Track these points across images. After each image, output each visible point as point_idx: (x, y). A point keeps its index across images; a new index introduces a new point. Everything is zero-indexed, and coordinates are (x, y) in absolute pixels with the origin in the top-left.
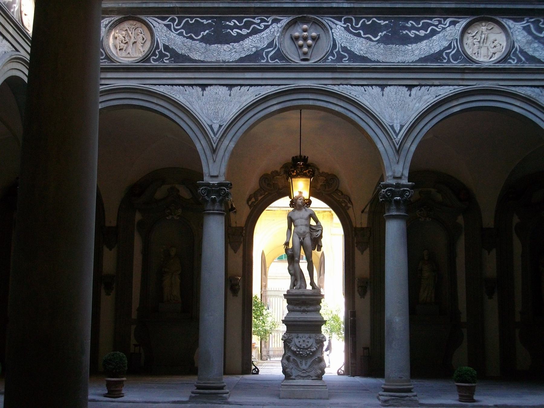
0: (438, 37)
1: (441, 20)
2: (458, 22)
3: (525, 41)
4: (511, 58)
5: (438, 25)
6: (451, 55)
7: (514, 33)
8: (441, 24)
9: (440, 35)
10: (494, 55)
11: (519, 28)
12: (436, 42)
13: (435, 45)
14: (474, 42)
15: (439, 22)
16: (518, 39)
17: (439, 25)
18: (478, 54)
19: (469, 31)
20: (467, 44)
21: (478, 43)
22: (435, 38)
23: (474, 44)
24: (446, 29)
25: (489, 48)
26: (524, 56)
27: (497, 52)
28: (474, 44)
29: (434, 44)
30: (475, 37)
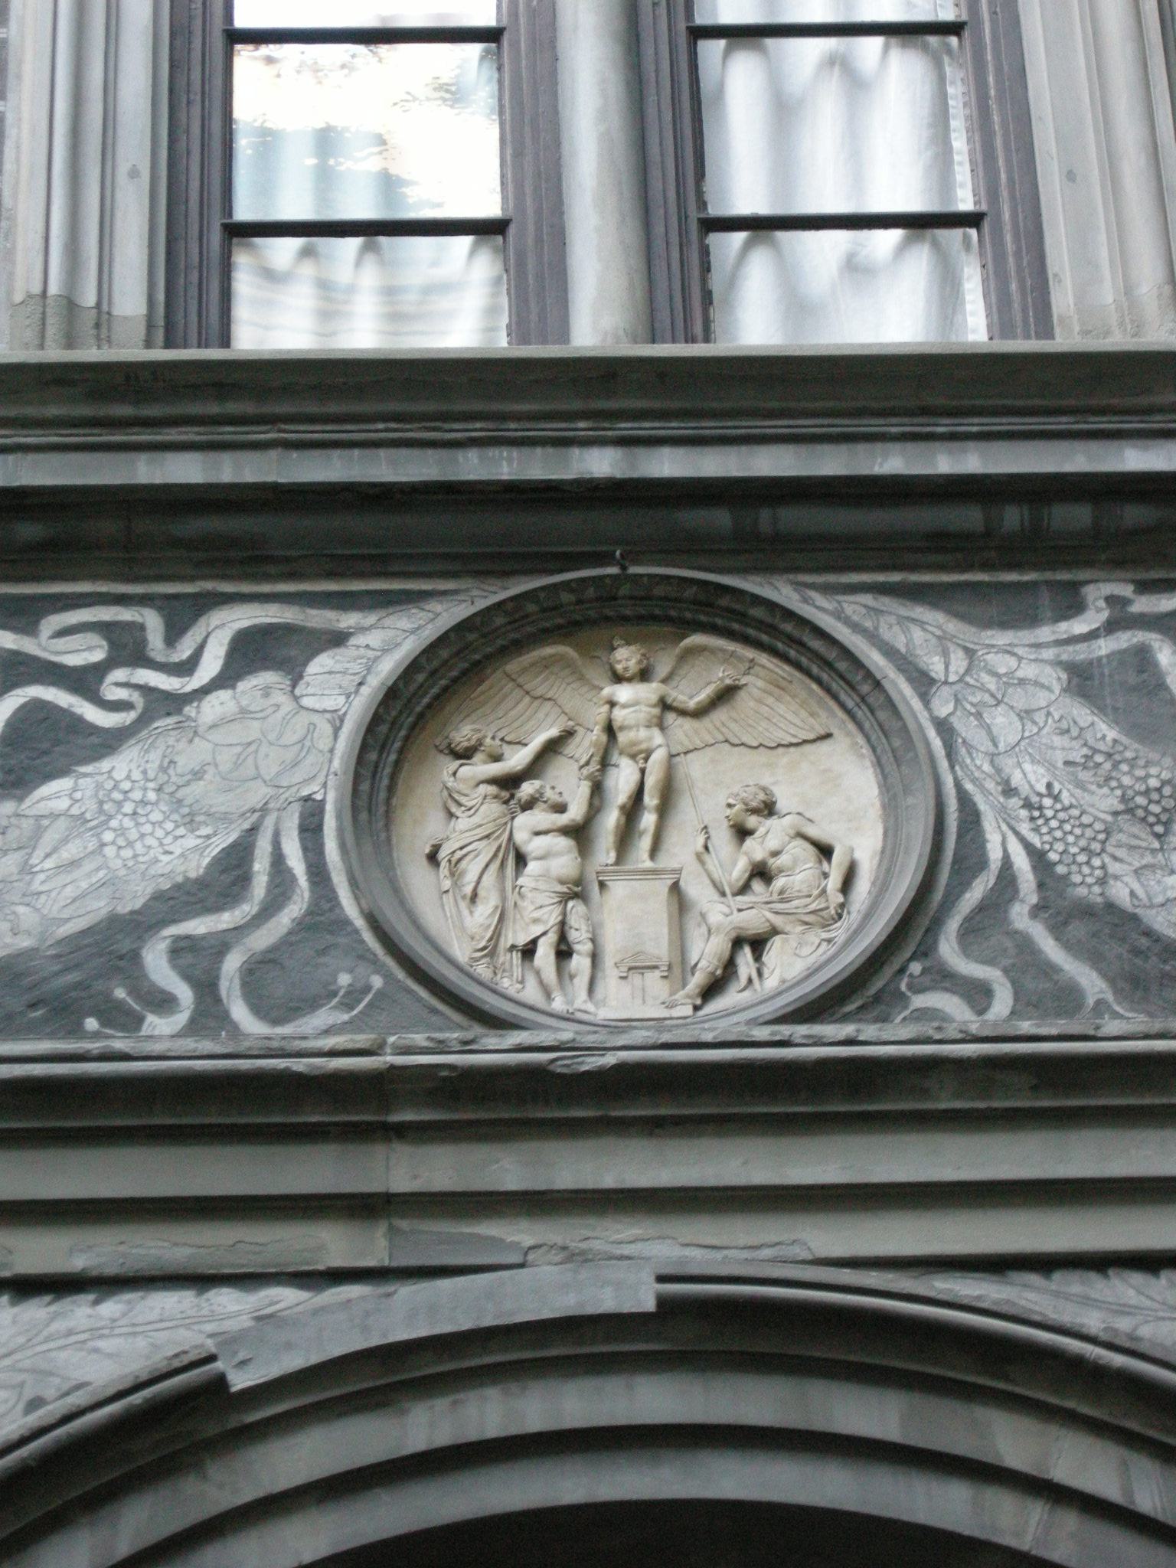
0: (99, 786)
1: (142, 627)
2: (338, 639)
3: (1103, 802)
4: (945, 979)
5: (99, 671)
6: (232, 964)
7: (967, 728)
8: (140, 658)
9: (122, 765)
10: (745, 959)
11: (1022, 682)
12: (65, 841)
13: (49, 864)
14: (520, 837)
15: (114, 645)
16: (1017, 779)
17: (119, 674)
18: (564, 952)
19: (463, 734)
20: (443, 854)
21: (564, 843)
22: (57, 796)
23: (521, 860)
24: (189, 710)
25: (697, 890)
26: (1095, 959)
27: (778, 921)
28: (521, 860)
29: (39, 853)
30: (527, 789)
